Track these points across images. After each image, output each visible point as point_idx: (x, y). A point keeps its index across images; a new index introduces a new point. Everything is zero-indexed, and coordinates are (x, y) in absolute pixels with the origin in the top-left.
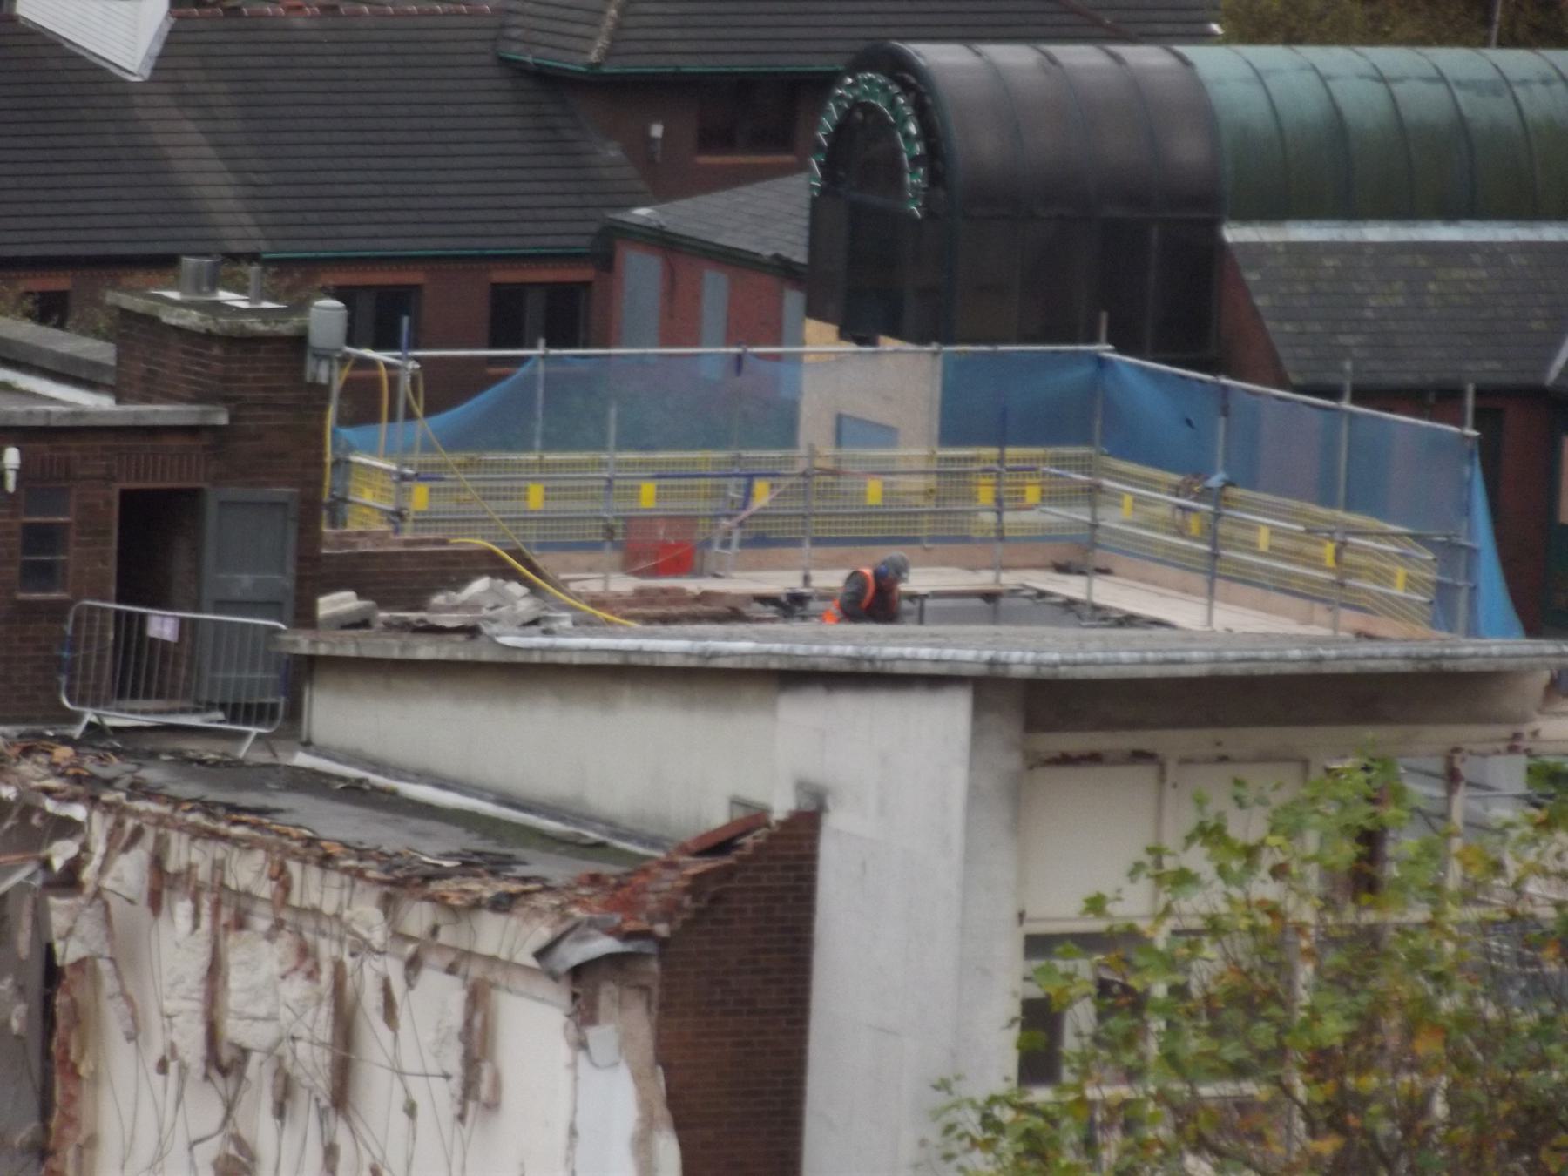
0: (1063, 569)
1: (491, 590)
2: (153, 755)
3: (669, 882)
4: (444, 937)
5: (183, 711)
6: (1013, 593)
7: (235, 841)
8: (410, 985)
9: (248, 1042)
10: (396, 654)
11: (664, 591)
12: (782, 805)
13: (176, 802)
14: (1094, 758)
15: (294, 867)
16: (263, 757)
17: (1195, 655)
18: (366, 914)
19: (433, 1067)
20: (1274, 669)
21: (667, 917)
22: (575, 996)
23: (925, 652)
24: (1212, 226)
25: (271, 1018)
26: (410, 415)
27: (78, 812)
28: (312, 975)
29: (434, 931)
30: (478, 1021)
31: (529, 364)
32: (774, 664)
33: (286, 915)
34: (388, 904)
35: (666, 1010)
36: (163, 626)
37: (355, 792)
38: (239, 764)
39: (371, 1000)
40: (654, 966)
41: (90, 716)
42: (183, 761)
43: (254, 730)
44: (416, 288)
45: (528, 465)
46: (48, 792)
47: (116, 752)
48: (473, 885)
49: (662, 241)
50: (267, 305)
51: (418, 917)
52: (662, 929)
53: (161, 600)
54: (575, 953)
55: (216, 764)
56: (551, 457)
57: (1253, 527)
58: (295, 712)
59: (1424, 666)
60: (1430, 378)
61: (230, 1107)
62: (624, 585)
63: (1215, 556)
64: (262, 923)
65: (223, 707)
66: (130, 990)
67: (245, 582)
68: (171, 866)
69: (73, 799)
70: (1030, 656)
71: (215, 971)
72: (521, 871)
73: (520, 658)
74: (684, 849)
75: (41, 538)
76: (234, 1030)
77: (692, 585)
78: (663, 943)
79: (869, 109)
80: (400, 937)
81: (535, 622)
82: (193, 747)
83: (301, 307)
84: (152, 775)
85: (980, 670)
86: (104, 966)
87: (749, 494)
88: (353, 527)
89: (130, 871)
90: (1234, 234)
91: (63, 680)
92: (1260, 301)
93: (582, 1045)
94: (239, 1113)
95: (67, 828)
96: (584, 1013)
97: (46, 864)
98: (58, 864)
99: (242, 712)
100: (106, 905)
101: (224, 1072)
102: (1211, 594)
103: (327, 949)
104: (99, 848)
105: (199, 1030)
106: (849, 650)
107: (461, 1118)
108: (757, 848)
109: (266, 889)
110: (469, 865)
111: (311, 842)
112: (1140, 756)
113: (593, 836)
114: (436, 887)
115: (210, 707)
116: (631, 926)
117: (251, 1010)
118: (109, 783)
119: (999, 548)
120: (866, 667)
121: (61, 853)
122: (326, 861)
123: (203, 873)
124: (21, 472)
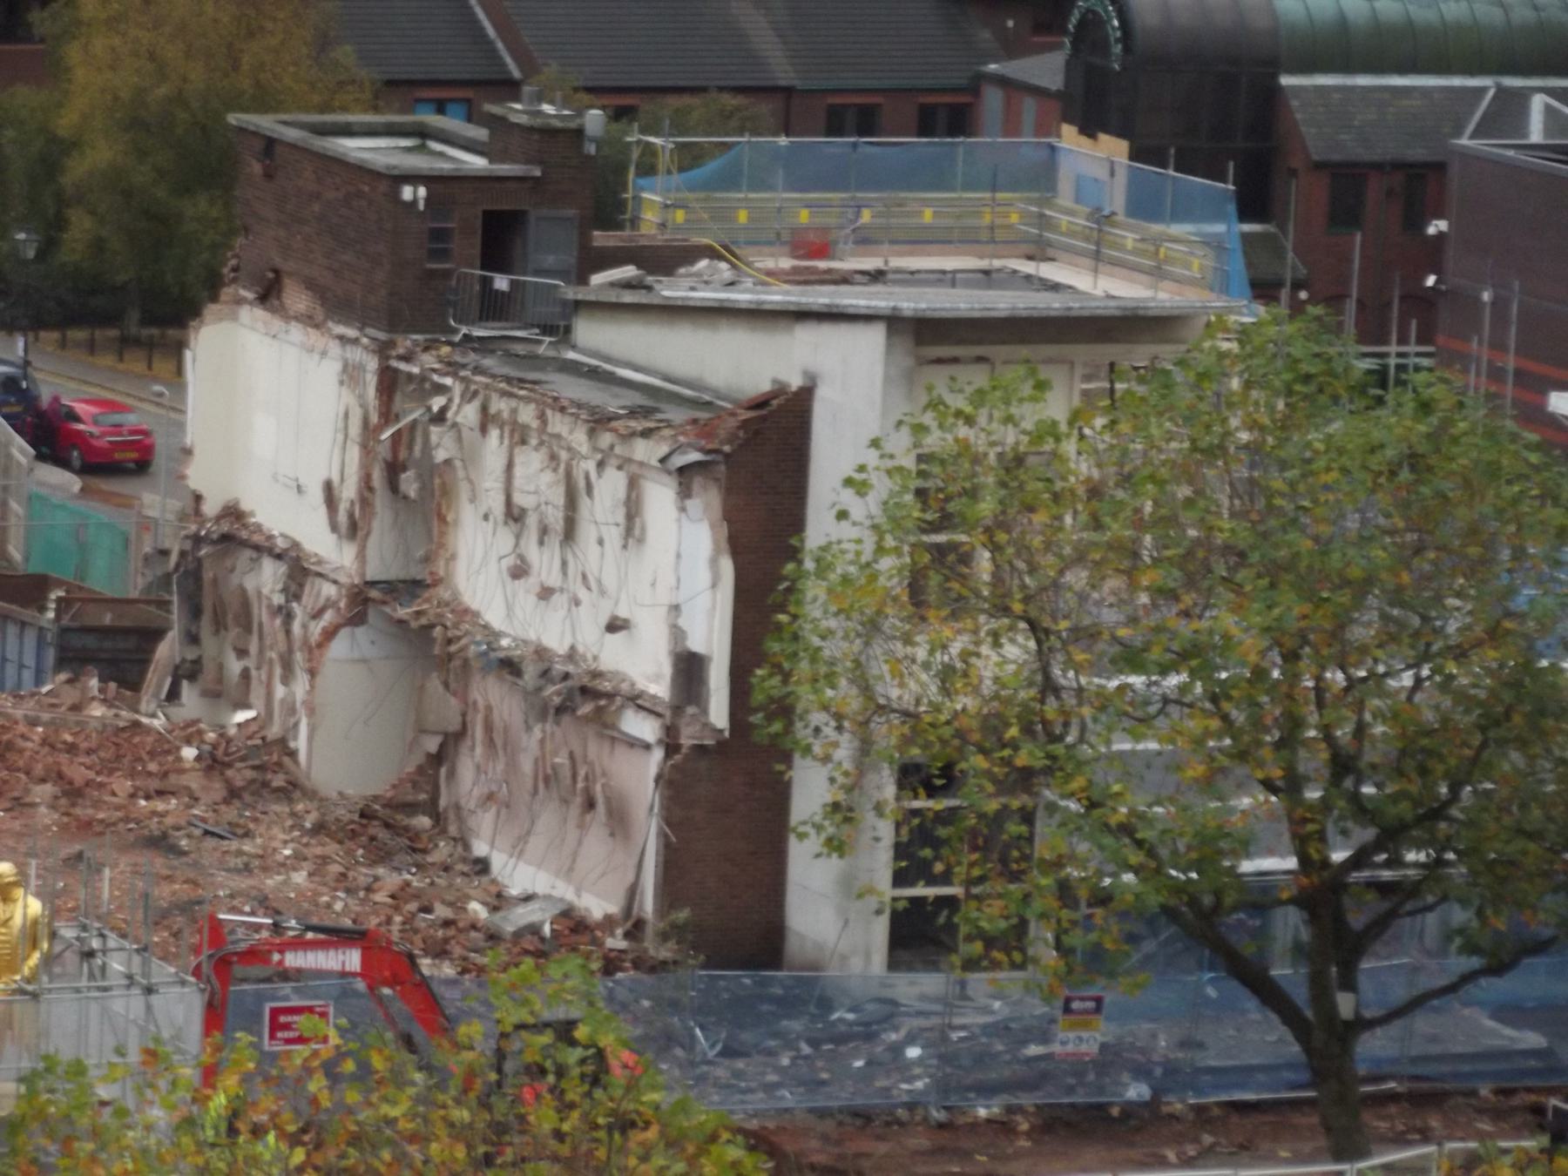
0: (1030, 258)
1: (709, 266)
2: (493, 352)
3: (732, 423)
4: (618, 450)
5: (519, 328)
6: (999, 270)
7: (521, 398)
8: (600, 475)
9: (525, 506)
10: (614, 300)
11: (807, 268)
12: (795, 382)
13: (493, 376)
14: (955, 360)
15: (549, 412)
16: (551, 353)
17: (1002, 306)
18: (579, 438)
19: (611, 520)
20: (1045, 313)
21: (729, 442)
22: (680, 484)
23: (862, 302)
24: (1274, 76)
25: (535, 493)
26: (669, 172)
27: (448, 381)
28: (555, 470)
29: (612, 447)
30: (634, 495)
31: (738, 148)
32: (792, 308)
33: (545, 438)
34: (592, 433)
35: (729, 491)
36: (501, 283)
37: (593, 374)
38: (537, 357)
39: (582, 484)
40: (723, 468)
41: (464, 330)
42: (510, 356)
43: (548, 339)
44: (879, 105)
45: (739, 200)
46: (434, 370)
47: (474, 350)
48: (633, 424)
49: (1003, 82)
50: (566, 112)
51: (606, 439)
52: (727, 448)
53: (503, 269)
54: (680, 460)
55: (524, 357)
56: (752, 195)
57: (1124, 237)
58: (568, 330)
59: (1128, 313)
60: (1388, 157)
61: (518, 537)
62: (786, 263)
63: (1098, 252)
64: (534, 442)
65: (538, 326)
66: (473, 477)
67: (550, 260)
68: (493, 410)
69: (446, 374)
70: (912, 305)
71: (510, 467)
72: (659, 416)
73: (672, 303)
74: (737, 403)
75: (439, 235)
76: (519, 499)
77: (822, 264)
78: (727, 456)
79: (1095, 13)
80: (595, 449)
81: (732, 284)
82: (520, 349)
83: (580, 113)
84: (488, 362)
85: (888, 312)
86: (458, 463)
87: (858, 215)
88: (643, 231)
89: (468, 414)
90: (1286, 80)
91: (451, 311)
92: (1298, 116)
93: (683, 509)
94: (522, 542)
95: (441, 389)
96: (685, 492)
97: (429, 409)
98: (435, 409)
99: (547, 329)
100: (459, 432)
101: (516, 520)
102: (1096, 271)
103: (564, 455)
104: (457, 400)
105: (501, 498)
106: (826, 301)
107: (625, 547)
108: (780, 406)
109: (535, 424)
110: (633, 413)
111: (556, 399)
112: (980, 359)
113: (707, 398)
114: (614, 424)
115: (533, 326)
116: (710, 446)
117: (526, 488)
118: (464, 366)
119: (991, 246)
120: (835, 310)
121: (437, 403)
122: (562, 410)
123: (506, 415)
124: (428, 200)
